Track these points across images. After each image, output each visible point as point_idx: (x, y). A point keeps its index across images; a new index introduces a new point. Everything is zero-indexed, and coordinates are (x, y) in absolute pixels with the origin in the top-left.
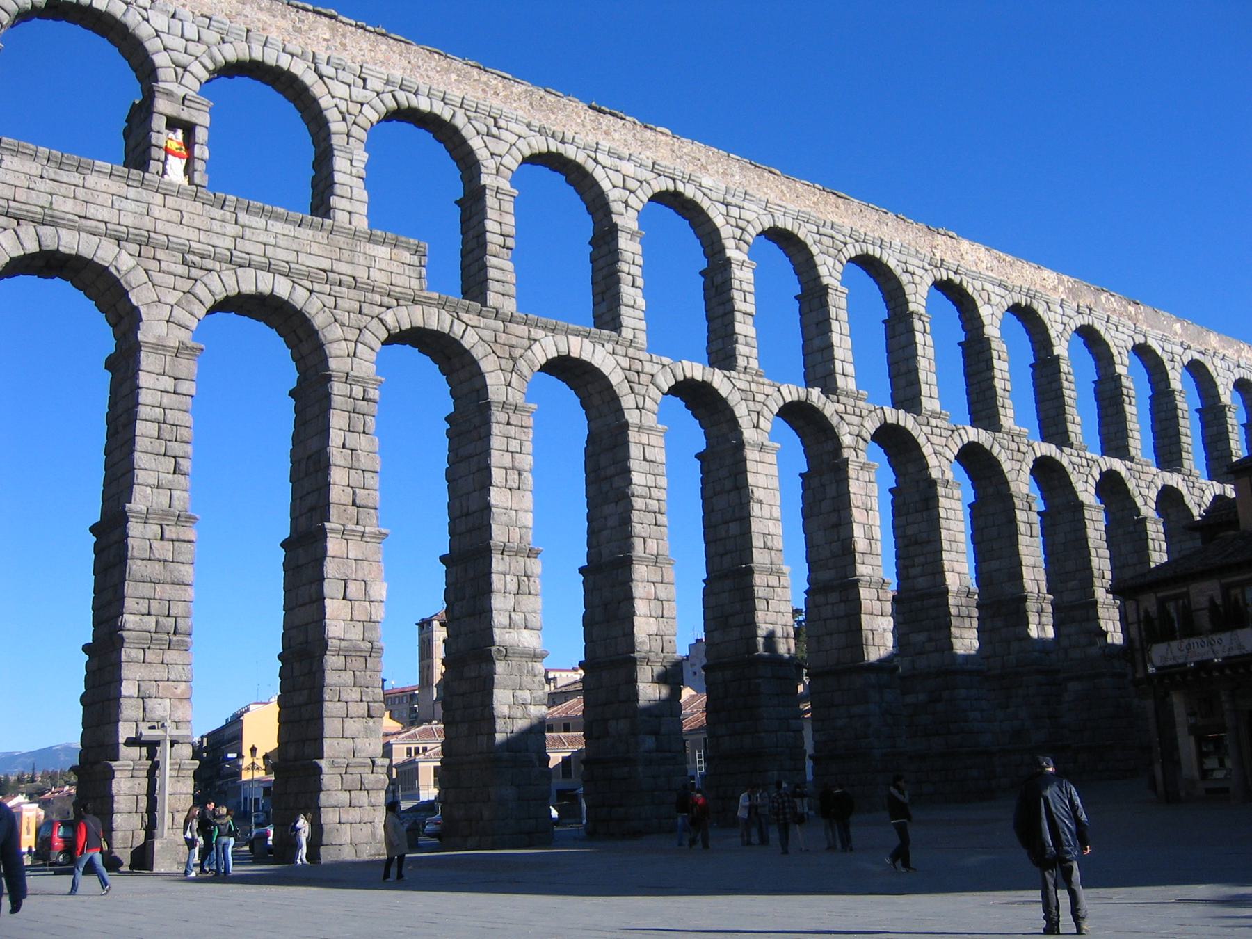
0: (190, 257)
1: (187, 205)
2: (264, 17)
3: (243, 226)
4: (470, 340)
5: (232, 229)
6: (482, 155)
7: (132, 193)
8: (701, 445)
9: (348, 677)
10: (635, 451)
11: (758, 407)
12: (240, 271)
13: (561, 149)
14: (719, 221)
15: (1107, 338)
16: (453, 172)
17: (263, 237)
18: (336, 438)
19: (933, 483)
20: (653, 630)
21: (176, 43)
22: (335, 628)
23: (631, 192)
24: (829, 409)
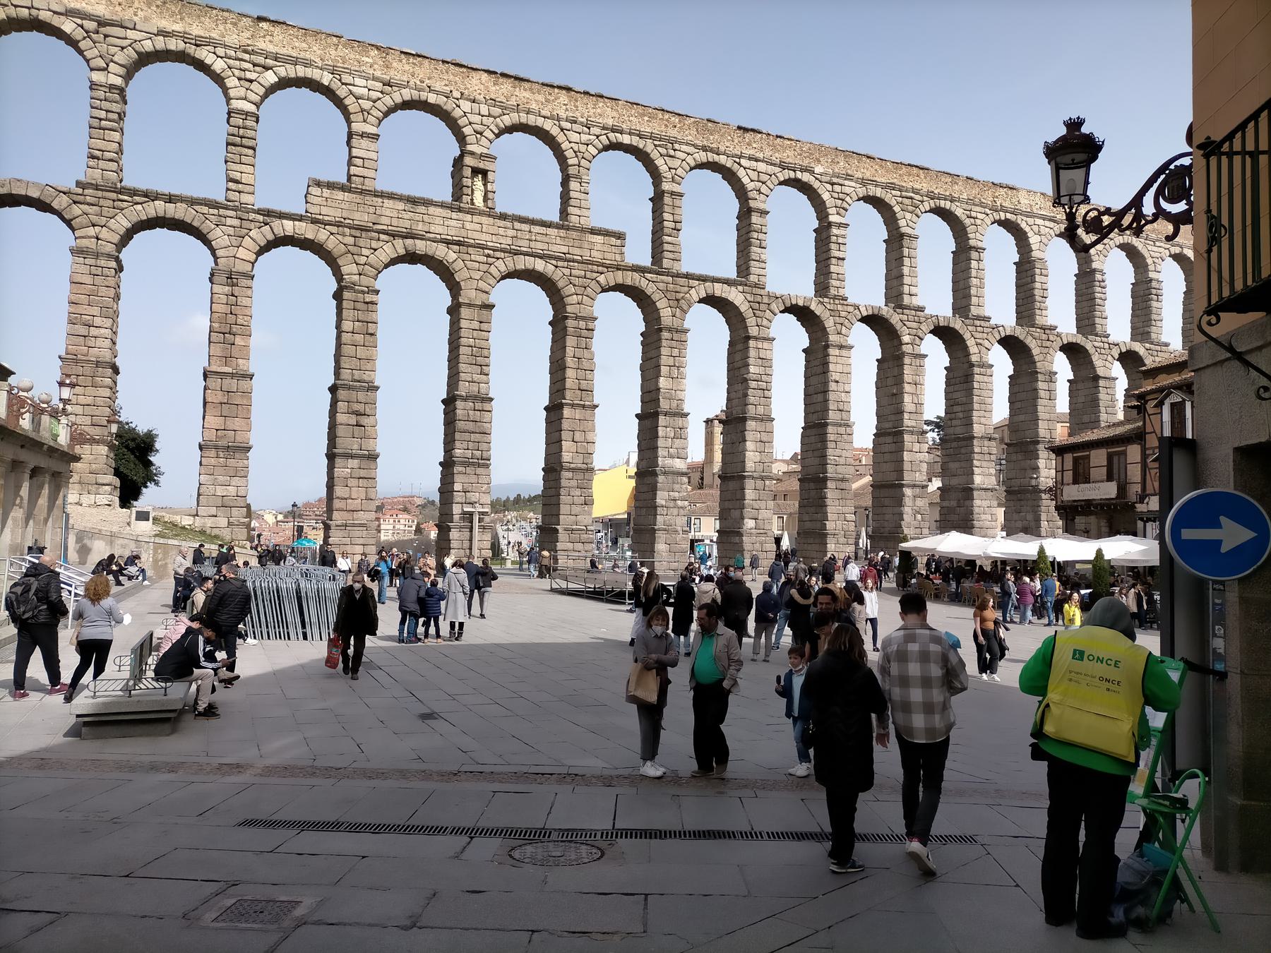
1: (485, 220)
2: (527, 94)
4: (650, 289)
5: (511, 233)
6: (663, 168)
7: (454, 215)
8: (806, 344)
9: (574, 483)
10: (752, 353)
11: (841, 320)
13: (716, 158)
14: (826, 196)
16: (648, 180)
18: (570, 351)
19: (972, 365)
20: (758, 459)
21: (477, 119)
22: (566, 457)
24: (895, 319)
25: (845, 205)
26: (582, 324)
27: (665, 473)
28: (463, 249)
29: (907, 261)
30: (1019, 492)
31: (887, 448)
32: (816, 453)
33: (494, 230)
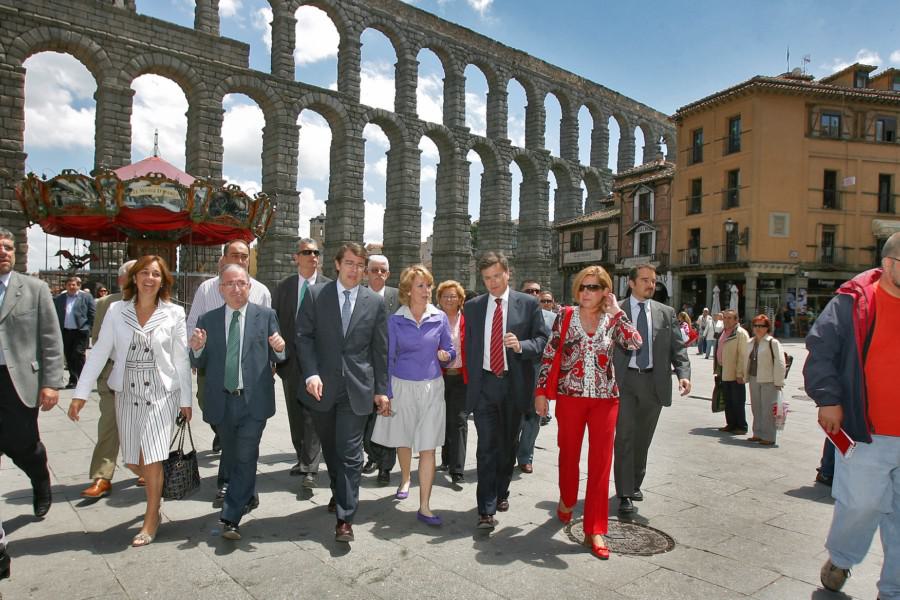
0: (128, 46)
1: (125, 19)
3: (156, 32)
5: (149, 33)
7: (98, 12)
10: (349, 149)
12: (155, 54)
15: (600, 109)
17: (165, 38)
18: (202, 135)
19: (499, 173)
20: (353, 230)
23: (359, 22)
24: (451, 134)
25: (417, 48)
26: (212, 115)
27: (280, 239)
28: (106, 42)
29: (458, 95)
30: (524, 262)
31: (442, 228)
32: (396, 229)
33: (135, 29)
